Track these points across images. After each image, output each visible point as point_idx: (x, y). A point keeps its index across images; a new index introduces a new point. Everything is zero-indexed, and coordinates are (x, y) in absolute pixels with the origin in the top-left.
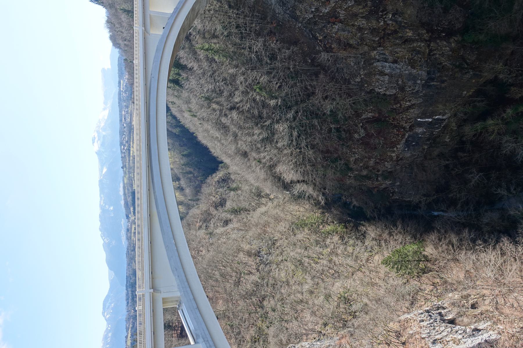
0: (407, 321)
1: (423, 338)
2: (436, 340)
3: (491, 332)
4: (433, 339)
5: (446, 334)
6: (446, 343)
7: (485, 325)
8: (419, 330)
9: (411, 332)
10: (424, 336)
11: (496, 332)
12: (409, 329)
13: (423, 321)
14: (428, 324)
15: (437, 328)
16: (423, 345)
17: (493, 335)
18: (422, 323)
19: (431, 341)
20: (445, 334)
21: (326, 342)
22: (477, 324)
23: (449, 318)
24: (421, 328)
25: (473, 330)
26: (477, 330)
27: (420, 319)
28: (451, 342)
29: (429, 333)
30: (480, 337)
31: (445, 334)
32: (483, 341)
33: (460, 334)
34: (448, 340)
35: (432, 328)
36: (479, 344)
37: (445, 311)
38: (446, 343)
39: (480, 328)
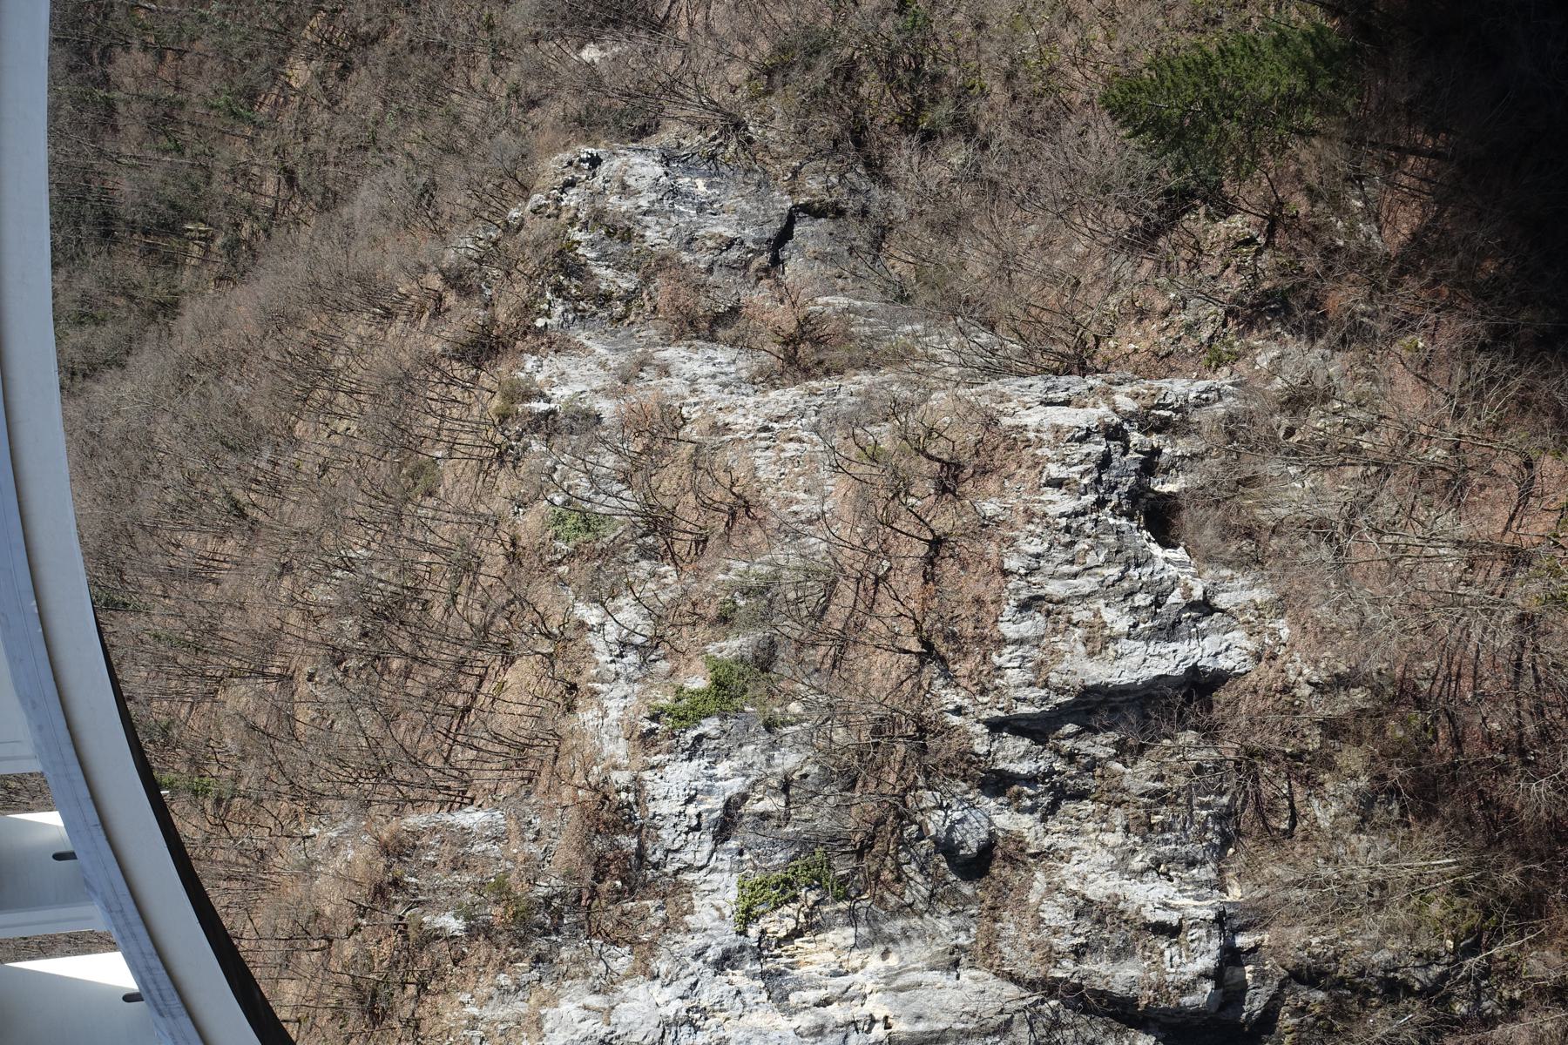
0: (1016, 441)
1: (1006, 573)
2: (1041, 598)
3: (1238, 637)
4: (1035, 591)
5: (1087, 590)
6: (1061, 626)
7: (1244, 597)
8: (1019, 520)
9: (990, 508)
10: (1012, 563)
11: (1251, 645)
12: (992, 485)
13: (1058, 484)
14: (1062, 515)
15: (1082, 545)
16: (988, 598)
17: (1233, 653)
18: (1051, 494)
19: (1024, 595)
20: (1085, 584)
21: (733, 199)
22: (1226, 572)
23: (1168, 488)
24: (1030, 516)
25: (1191, 606)
26: (1205, 607)
27: (1054, 470)
28: (1078, 632)
29: (1038, 556)
30: (1183, 648)
31: (1085, 584)
32: (1182, 669)
33: (1134, 610)
34: (1075, 618)
35: (1067, 538)
36: (1160, 676)
37: (1183, 446)
38: (1061, 626)
39: (1221, 600)
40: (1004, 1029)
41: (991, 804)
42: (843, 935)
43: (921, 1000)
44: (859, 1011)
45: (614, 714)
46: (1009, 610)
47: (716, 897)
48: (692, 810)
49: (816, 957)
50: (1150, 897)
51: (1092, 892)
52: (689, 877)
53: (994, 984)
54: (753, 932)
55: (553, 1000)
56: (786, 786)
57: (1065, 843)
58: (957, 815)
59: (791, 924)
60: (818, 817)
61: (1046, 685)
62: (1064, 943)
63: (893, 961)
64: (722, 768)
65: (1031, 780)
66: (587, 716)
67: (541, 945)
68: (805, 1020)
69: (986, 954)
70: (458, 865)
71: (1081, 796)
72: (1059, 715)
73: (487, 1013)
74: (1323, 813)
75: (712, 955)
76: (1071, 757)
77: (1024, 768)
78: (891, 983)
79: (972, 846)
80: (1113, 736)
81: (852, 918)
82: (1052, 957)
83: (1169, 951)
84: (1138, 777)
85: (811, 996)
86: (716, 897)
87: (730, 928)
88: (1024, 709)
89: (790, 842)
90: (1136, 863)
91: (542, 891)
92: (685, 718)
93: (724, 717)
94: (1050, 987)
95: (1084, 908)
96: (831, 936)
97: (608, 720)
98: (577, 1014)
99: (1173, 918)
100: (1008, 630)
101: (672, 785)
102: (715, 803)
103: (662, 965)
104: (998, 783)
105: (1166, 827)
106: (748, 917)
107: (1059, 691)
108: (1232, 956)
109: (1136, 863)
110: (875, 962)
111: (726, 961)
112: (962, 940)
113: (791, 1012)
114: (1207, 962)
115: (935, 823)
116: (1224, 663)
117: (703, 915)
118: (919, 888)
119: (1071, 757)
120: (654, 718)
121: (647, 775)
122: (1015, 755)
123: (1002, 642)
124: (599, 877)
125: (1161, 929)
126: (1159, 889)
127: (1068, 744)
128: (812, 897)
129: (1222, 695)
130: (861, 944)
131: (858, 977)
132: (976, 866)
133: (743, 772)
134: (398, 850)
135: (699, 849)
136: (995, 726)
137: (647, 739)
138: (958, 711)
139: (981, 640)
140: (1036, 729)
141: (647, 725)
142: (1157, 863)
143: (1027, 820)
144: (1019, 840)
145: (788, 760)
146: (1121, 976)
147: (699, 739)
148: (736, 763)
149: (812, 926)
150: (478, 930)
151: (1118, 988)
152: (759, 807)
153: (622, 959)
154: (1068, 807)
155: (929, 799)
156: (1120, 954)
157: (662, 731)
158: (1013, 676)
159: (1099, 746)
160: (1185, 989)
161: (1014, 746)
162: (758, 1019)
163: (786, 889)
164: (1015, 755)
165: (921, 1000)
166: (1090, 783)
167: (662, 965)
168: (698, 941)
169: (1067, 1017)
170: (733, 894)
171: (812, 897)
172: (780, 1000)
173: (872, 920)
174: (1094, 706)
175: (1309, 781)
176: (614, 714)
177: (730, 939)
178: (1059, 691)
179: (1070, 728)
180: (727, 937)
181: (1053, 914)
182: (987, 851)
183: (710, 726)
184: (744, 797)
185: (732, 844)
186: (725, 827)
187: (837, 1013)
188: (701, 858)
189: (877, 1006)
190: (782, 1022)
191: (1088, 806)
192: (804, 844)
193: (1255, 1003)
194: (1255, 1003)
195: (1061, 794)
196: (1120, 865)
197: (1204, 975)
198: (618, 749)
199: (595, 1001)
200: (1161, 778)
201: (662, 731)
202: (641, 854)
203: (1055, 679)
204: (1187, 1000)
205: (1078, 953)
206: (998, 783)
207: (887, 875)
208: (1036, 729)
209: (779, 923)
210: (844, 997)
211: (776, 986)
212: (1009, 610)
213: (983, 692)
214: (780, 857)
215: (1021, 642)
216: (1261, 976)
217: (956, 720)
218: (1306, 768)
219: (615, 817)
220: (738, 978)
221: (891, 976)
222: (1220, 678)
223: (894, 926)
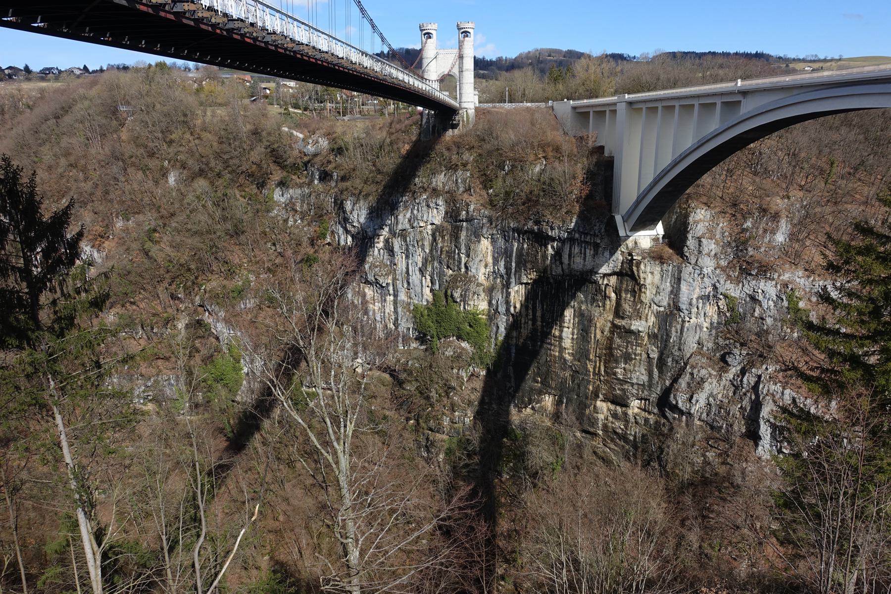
30: (768, 437)
40: (680, 349)
41: (739, 368)
42: (715, 319)
43: (692, 332)
44: (693, 316)
45: (798, 280)
46: (794, 394)
47: (734, 291)
48: (760, 291)
49: (711, 310)
50: (701, 399)
51: (706, 385)
52: (741, 285)
53: (691, 351)
54: (721, 297)
55: (717, 243)
56: (762, 319)
57: (722, 383)
58: (737, 357)
59: (722, 307)
60: (750, 324)
61: (767, 395)
62: (695, 371)
63: (705, 329)
64: (771, 303)
65: (741, 381)
66: (801, 273)
67: (734, 244)
68: (694, 301)
69: (699, 352)
70: (765, 231)
71: (734, 393)
72: (757, 396)
73: (719, 228)
74: (710, 455)
75: (717, 284)
76: (745, 394)
77: (745, 379)
78: (699, 326)
79: (729, 360)
80: (748, 409)
81: (718, 323)
82: (693, 367)
83: (685, 397)
84: (735, 409)
85: (700, 305)
86: (734, 291)
87: (723, 291)
88: (761, 386)
89: (745, 314)
90: (711, 399)
91: (749, 249)
92: (790, 298)
93: (788, 308)
94: (686, 364)
95: (703, 380)
96: (716, 317)
97: (799, 279)
98: (710, 248)
99: (694, 401)
100: (787, 392)
101: (768, 289)
102: (761, 298)
103: (718, 271)
104: (743, 372)
105: (719, 412)
106: (726, 297)
107: (764, 398)
108: (681, 413)
109: (711, 399)
110: (705, 325)
111: (715, 288)
112: (705, 348)
113: (697, 299)
114: (680, 405)
115: (736, 351)
116: (760, 448)
117: (728, 285)
118: (721, 341)
119: (745, 394)
120: (792, 289)
121: (774, 283)
122: (749, 379)
123: (784, 389)
124: (748, 262)
125: (692, 397)
126: (702, 402)
127: (749, 395)
128: (728, 315)
129: (752, 443)
130: (711, 324)
131: (703, 319)
132: (723, 359)
133: (768, 308)
134: (776, 217)
135: (748, 290)
136: (759, 377)
137: (786, 285)
138: (767, 369)
139: (787, 383)
140: (755, 388)
141: (790, 287)
142: (710, 405)
143: (732, 377)
144: (726, 372)
145: (769, 321)
146: (683, 383)
147: (782, 299)
148: (772, 307)
149: (720, 312)
150: (744, 230)
151: (680, 380)
152: (757, 310)
153: (723, 263)
154: (733, 389)
155: (744, 352)
156: (689, 384)
157: (787, 291)
158: (772, 387)
159: (746, 403)
160: (675, 398)
161: (753, 381)
162: (697, 290)
163: (731, 309)
164: (749, 379)
165: (692, 332)
166: (737, 396)
167: (718, 271)
168: (722, 282)
169: (678, 366)
170: (733, 294)
171: (728, 315)
172: (701, 297)
173: (717, 328)
174: (757, 406)
175: (720, 455)
176: (798, 280)
177: (721, 290)
178: (764, 398)
179: (753, 397)
180: (721, 290)
181: (703, 372)
182: (726, 363)
183: (785, 304)
184: (761, 306)
185: (748, 299)
186: (753, 299)
187: (694, 310)
188: (745, 289)
189: (693, 320)
190: (695, 296)
191: (731, 394)
192: (743, 318)
193: (669, 413)
194: (669, 413)
195: (737, 388)
196: (711, 395)
197: (677, 402)
198: (786, 277)
199: (713, 253)
200: (733, 416)
201: (787, 291)
202: (750, 274)
203: (767, 398)
204: (672, 395)
205: (692, 374)
206: (743, 372)
207: (728, 335)
208: (755, 388)
209: (722, 303)
210: (698, 313)
211: (705, 298)
212: (794, 394)
213: (770, 377)
214: (741, 310)
215: (783, 393)
216: (674, 418)
217: (764, 367)
218: (724, 454)
219: (764, 270)
220: (710, 289)
221: (701, 328)
222: (757, 445)
223: (714, 332)
